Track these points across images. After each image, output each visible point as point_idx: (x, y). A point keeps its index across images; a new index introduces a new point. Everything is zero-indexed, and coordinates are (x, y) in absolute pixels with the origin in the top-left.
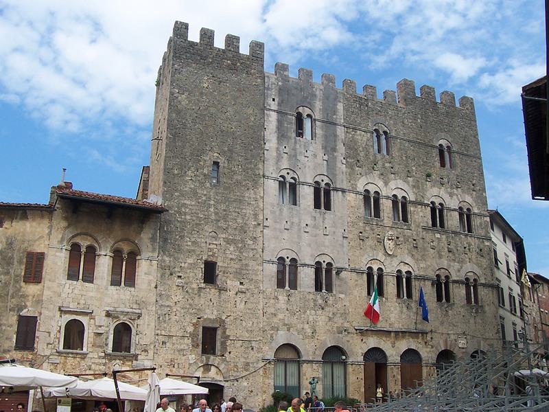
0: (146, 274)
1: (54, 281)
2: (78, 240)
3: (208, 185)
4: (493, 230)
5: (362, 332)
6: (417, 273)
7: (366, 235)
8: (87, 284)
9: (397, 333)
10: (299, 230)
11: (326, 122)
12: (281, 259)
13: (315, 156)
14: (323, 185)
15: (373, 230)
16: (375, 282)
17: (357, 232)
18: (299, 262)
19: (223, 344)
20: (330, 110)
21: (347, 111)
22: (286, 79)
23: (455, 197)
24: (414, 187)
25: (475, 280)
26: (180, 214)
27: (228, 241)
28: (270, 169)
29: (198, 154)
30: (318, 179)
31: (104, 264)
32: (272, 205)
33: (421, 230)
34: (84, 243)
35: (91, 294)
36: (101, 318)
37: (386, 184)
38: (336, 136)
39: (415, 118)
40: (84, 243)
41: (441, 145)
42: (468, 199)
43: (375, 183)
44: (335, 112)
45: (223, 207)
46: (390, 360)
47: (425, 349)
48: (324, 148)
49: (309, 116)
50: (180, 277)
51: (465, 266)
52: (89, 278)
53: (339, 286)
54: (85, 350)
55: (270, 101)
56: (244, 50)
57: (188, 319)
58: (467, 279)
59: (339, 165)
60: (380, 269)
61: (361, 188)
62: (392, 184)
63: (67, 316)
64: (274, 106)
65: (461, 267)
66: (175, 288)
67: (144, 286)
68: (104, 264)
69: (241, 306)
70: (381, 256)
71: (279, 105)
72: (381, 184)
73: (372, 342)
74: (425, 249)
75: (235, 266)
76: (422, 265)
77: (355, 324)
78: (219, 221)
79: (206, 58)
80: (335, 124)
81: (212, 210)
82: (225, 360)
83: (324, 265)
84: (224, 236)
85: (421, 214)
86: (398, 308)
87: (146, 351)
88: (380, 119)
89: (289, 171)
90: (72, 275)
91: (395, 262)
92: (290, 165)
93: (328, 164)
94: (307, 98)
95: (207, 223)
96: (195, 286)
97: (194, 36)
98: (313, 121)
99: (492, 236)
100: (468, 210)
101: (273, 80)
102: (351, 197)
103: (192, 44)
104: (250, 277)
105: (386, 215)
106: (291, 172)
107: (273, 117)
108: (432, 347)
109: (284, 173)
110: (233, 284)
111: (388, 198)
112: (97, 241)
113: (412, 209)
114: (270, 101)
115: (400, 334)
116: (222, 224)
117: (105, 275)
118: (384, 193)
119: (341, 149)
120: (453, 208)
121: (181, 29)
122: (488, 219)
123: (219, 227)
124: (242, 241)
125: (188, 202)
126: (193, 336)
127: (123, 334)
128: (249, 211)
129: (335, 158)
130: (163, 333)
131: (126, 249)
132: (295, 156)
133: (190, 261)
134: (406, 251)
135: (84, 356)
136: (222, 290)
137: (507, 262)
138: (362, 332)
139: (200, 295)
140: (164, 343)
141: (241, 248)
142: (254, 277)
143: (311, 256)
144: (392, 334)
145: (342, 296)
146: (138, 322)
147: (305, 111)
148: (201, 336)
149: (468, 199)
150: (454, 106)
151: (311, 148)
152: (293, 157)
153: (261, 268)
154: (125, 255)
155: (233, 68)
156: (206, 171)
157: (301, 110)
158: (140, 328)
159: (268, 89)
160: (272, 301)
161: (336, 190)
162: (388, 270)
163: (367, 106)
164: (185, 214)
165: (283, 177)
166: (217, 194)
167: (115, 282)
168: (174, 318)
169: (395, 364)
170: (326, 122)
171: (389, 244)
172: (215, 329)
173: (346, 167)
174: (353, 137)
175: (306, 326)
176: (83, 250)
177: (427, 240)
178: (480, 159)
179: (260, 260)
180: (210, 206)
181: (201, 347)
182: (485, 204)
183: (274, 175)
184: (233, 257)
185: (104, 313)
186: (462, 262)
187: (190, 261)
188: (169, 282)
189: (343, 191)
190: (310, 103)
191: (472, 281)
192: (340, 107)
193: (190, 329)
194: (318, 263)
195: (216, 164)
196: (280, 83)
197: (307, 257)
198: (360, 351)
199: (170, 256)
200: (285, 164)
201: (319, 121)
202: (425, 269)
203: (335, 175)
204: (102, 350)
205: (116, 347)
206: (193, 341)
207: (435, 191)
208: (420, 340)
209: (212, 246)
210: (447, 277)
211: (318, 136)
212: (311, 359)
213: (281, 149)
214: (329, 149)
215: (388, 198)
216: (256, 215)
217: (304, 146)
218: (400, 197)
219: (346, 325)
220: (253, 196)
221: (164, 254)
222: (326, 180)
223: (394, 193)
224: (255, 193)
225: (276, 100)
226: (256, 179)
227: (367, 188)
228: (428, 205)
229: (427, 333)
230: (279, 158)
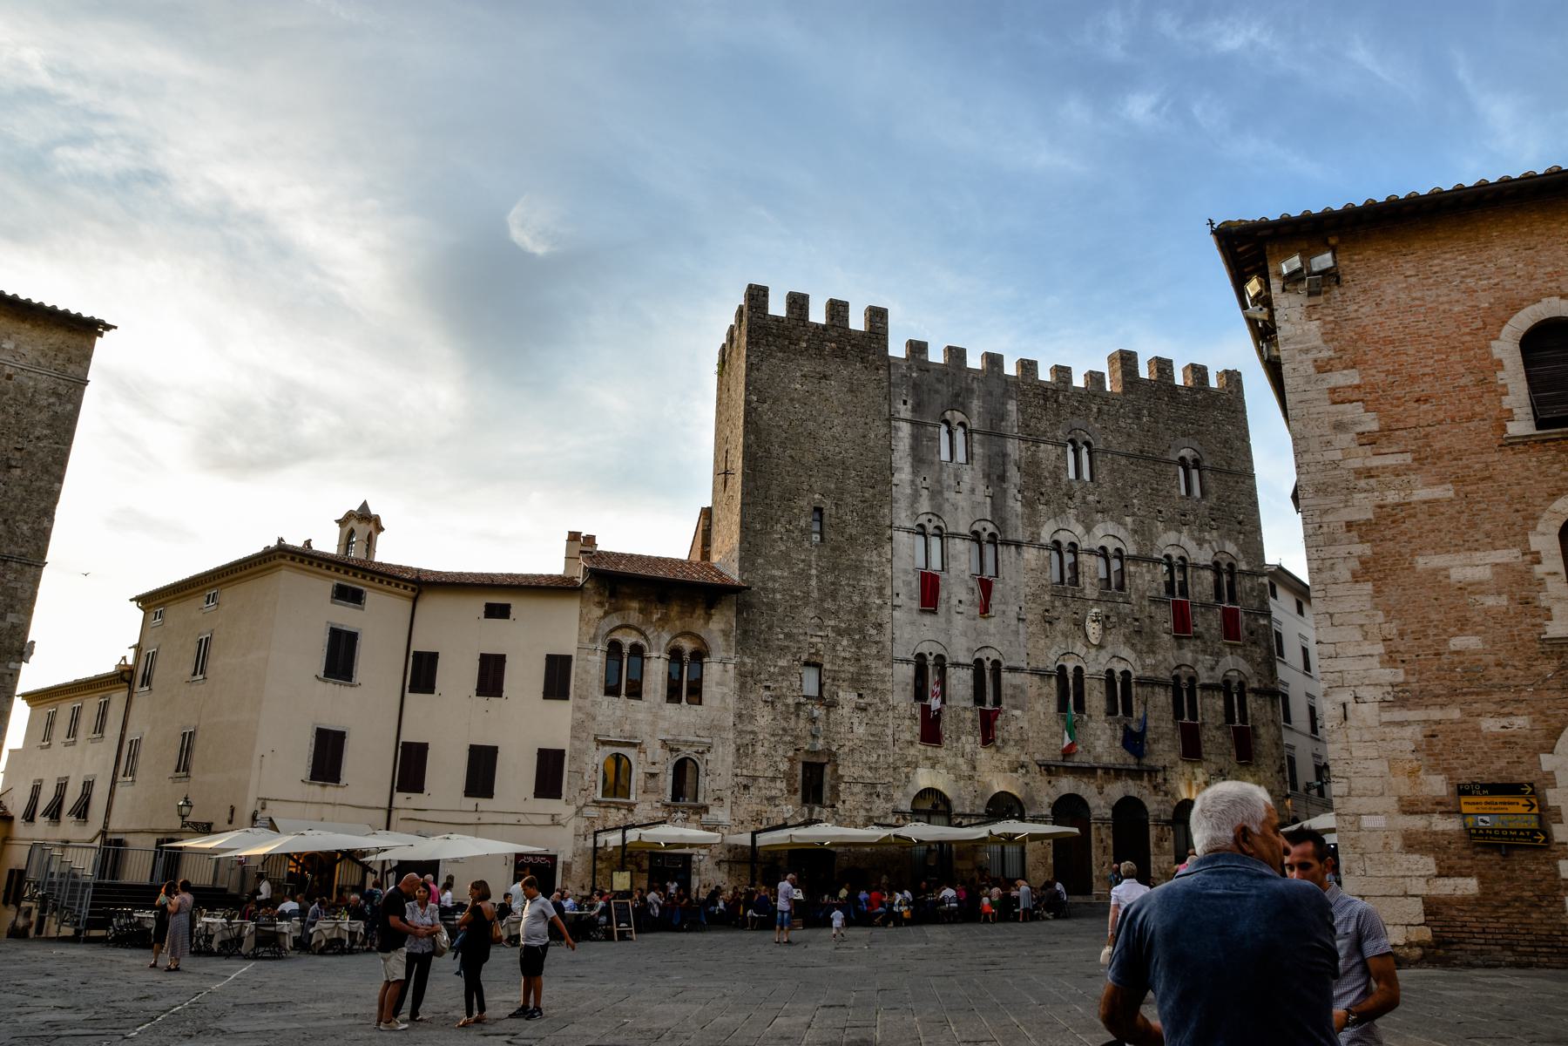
0: (718, 684)
1: (585, 698)
2: (617, 636)
3: (807, 544)
4: (1275, 596)
5: (1050, 770)
6: (1140, 673)
7: (1056, 614)
8: (632, 702)
9: (1106, 770)
10: (949, 610)
11: (990, 434)
12: (921, 656)
13: (973, 491)
14: (985, 536)
15: (1066, 605)
16: (1069, 690)
17: (1040, 610)
18: (948, 661)
19: (835, 790)
21: (1023, 413)
22: (926, 367)
23: (1206, 546)
24: (1135, 532)
25: (1241, 684)
26: (765, 589)
27: (839, 632)
28: (903, 518)
29: (789, 496)
30: (977, 527)
31: (656, 671)
32: (906, 572)
33: (1146, 603)
34: (628, 639)
35: (640, 716)
36: (656, 752)
37: (1088, 530)
38: (1005, 455)
39: (1138, 417)
40: (628, 639)
41: (1182, 459)
42: (1231, 548)
43: (1073, 531)
44: (1003, 417)
45: (830, 578)
46: (1095, 813)
47: (1154, 798)
48: (987, 476)
49: (962, 424)
50: (767, 688)
51: (1222, 661)
52: (635, 692)
53: (1013, 697)
54: (633, 798)
55: (901, 407)
56: (857, 322)
57: (781, 752)
58: (1227, 682)
59: (1011, 502)
60: (1078, 670)
61: (1046, 537)
62: (1099, 531)
63: (607, 748)
64: (905, 411)
65: (1217, 662)
66: (761, 704)
67: (716, 703)
68: (656, 671)
69: (860, 730)
70: (1079, 648)
71: (914, 410)
72: (1079, 529)
73: (1066, 785)
74: (1154, 635)
75: (851, 669)
76: (1148, 661)
77: (1037, 757)
78: (822, 601)
79: (799, 340)
80: (1003, 436)
81: (814, 582)
82: (837, 813)
83: (988, 664)
84: (832, 623)
85: (1148, 577)
86: (1109, 732)
87: (720, 799)
88: (1077, 422)
90: (612, 691)
91: (1104, 657)
92: (932, 507)
93: (993, 504)
94: (957, 395)
95: (806, 604)
96: (790, 701)
97: (777, 307)
98: (968, 433)
99: (1272, 608)
100: (1231, 565)
101: (904, 370)
102: (1030, 554)
103: (777, 319)
104: (874, 685)
105: (1088, 580)
107: (905, 430)
108: (1166, 794)
109: (923, 520)
110: (846, 696)
111: (1091, 552)
112: (646, 638)
113: (1132, 569)
115: (1114, 773)
116: (829, 604)
117: (659, 688)
118: (1084, 545)
119: (1014, 476)
120: (1203, 563)
121: (757, 296)
122: (1266, 580)
123: (825, 610)
124: (861, 630)
125: (777, 573)
126: (789, 777)
127: (684, 774)
128: (870, 583)
129: (1005, 491)
130: (745, 772)
131: (687, 646)
132: (941, 493)
133: (782, 663)
134: (1121, 639)
135: (630, 808)
136: (831, 705)
137: (1305, 651)
138: (1050, 770)
139: (798, 716)
140: (746, 787)
141: (859, 641)
142: (879, 686)
143: (969, 649)
144: (1099, 772)
145: (1018, 713)
146: (708, 756)
148: (800, 777)
149: (1231, 548)
150: (1208, 390)
151: (966, 478)
152: (936, 494)
153: (888, 671)
154: (686, 657)
155: (841, 354)
156: (803, 523)
157: (948, 415)
158: (710, 766)
159: (897, 385)
160: (907, 722)
161: (1007, 543)
162: (1092, 670)
164: (774, 591)
165: (921, 526)
166: (819, 557)
167: (673, 694)
168: (760, 750)
169: (1103, 820)
170: (990, 434)
171: (1093, 629)
172: (822, 766)
174: (1034, 454)
175: (961, 761)
176: (626, 650)
177: (1158, 617)
178: (1252, 476)
179: (888, 659)
180: (809, 577)
181: (799, 794)
182: (1260, 554)
183: (908, 525)
184: (847, 655)
185: (658, 744)
186: (1218, 655)
187: (782, 663)
188: (752, 696)
189: (1018, 545)
190: (962, 404)
191: (1235, 684)
192: (1012, 406)
193: (784, 766)
194: (979, 662)
195: (819, 510)
197: (961, 651)
198: (1046, 800)
199: (752, 655)
200: (925, 505)
201: (977, 432)
202: (1155, 667)
203: (1004, 521)
204: (654, 797)
205: (678, 793)
206: (789, 784)
207: (1172, 537)
208: (1145, 783)
209: (815, 640)
210: (1192, 680)
212: (968, 811)
214: (996, 477)
215: (1091, 552)
216: (880, 590)
217: (956, 476)
218: (1111, 550)
219: (1023, 758)
220: (875, 558)
221: (744, 653)
222: (990, 528)
223: (1103, 543)
224: (880, 555)
225: (910, 402)
226: (880, 535)
227: (1056, 537)
228: (1159, 561)
229: (1157, 771)
230: (915, 496)
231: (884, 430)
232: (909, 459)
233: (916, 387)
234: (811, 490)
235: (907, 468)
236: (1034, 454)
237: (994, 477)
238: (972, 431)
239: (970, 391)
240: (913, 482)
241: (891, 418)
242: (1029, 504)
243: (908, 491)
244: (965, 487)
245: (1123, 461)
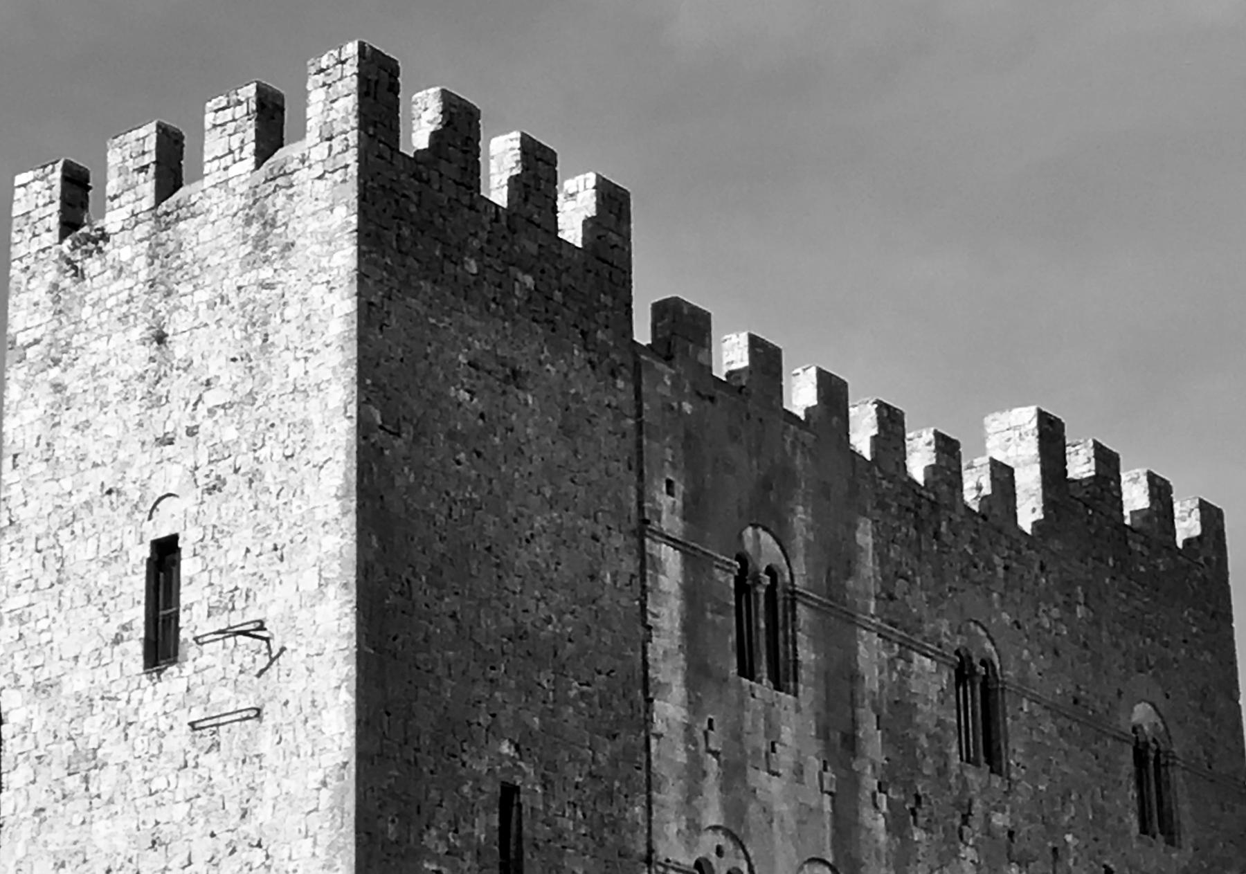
20: (837, 560)
38: (855, 678)
39: (1069, 606)
48: (823, 733)
55: (665, 501)
59: (867, 813)
89: (721, 839)
106: (729, 846)
114: (665, 501)
147: (764, 548)
163: (937, 535)
173: (888, 829)
192: (865, 537)
196: (687, 407)
211: (803, 674)
213: (699, 734)
214: (840, 743)
225: (679, 487)
231: (629, 565)
232: (681, 660)
233: (690, 442)
234: (494, 732)
235: (678, 691)
236: (902, 685)
237: (836, 737)
238: (794, 596)
239: (787, 474)
240: (688, 728)
241: (643, 528)
242: (897, 826)
243: (681, 757)
244: (784, 758)
245: (1048, 726)
